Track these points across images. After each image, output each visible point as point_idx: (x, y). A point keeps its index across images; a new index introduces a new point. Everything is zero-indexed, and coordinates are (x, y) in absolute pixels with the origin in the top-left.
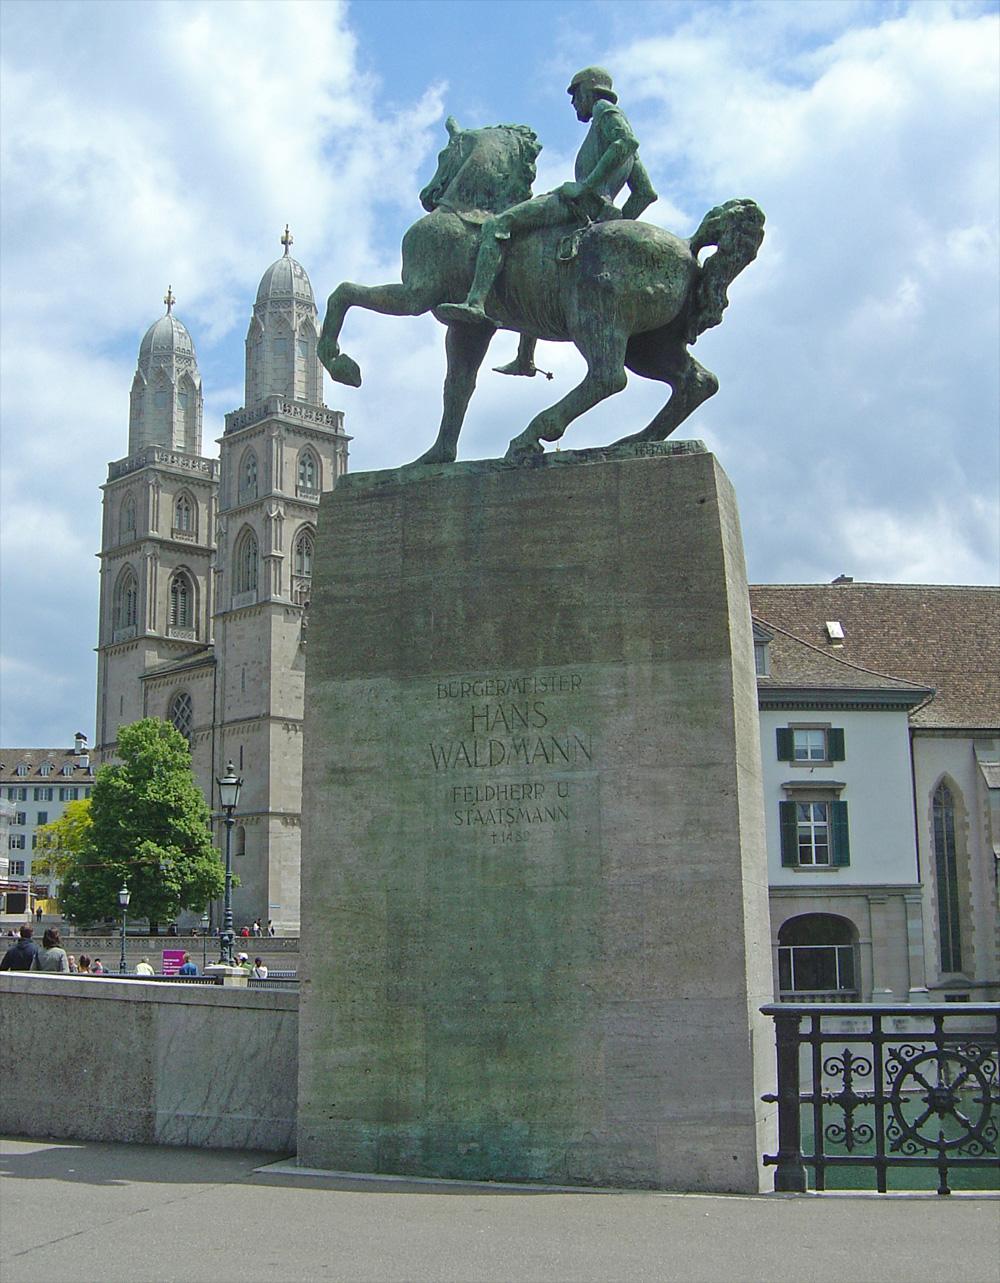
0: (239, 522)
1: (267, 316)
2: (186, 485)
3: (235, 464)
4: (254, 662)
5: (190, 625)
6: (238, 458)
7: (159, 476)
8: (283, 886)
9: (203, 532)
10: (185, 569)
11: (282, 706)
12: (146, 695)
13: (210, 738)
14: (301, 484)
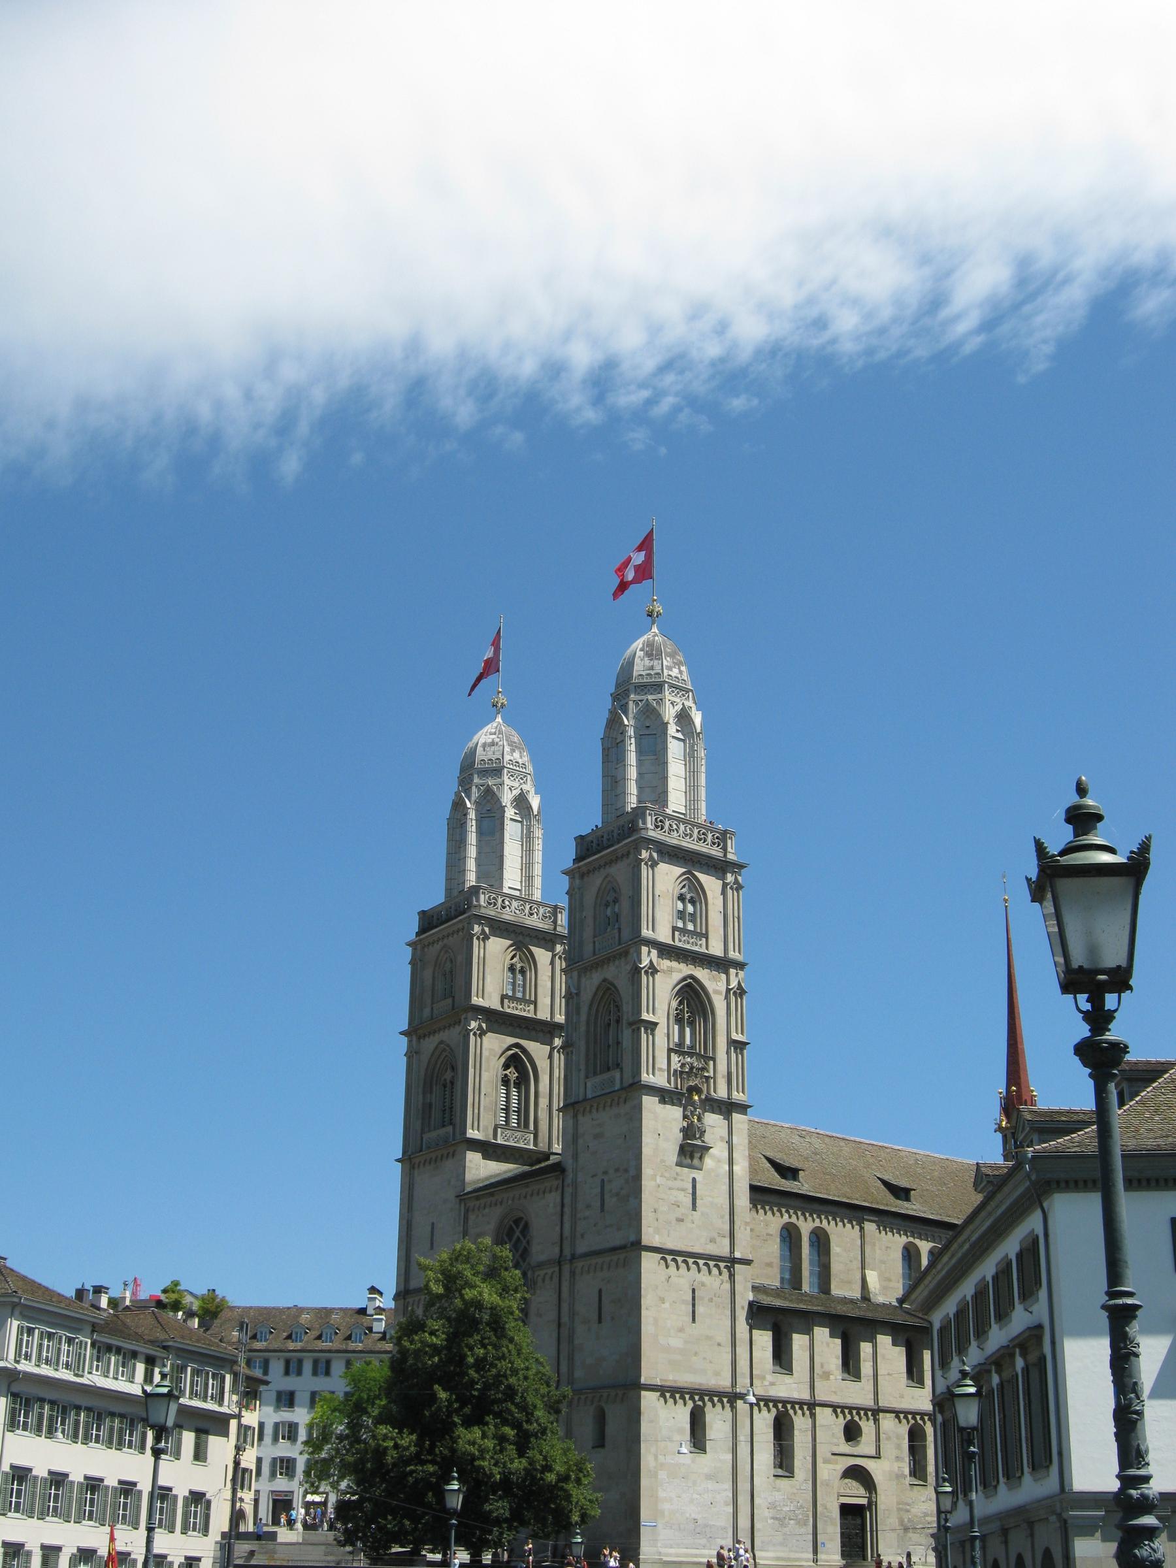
0: (596, 978)
1: (631, 703)
3: (590, 897)
4: (617, 1170)
5: (527, 1125)
6: (594, 890)
8: (661, 1494)
9: (544, 1001)
11: (657, 1231)
12: (466, 1219)
13: (556, 1280)
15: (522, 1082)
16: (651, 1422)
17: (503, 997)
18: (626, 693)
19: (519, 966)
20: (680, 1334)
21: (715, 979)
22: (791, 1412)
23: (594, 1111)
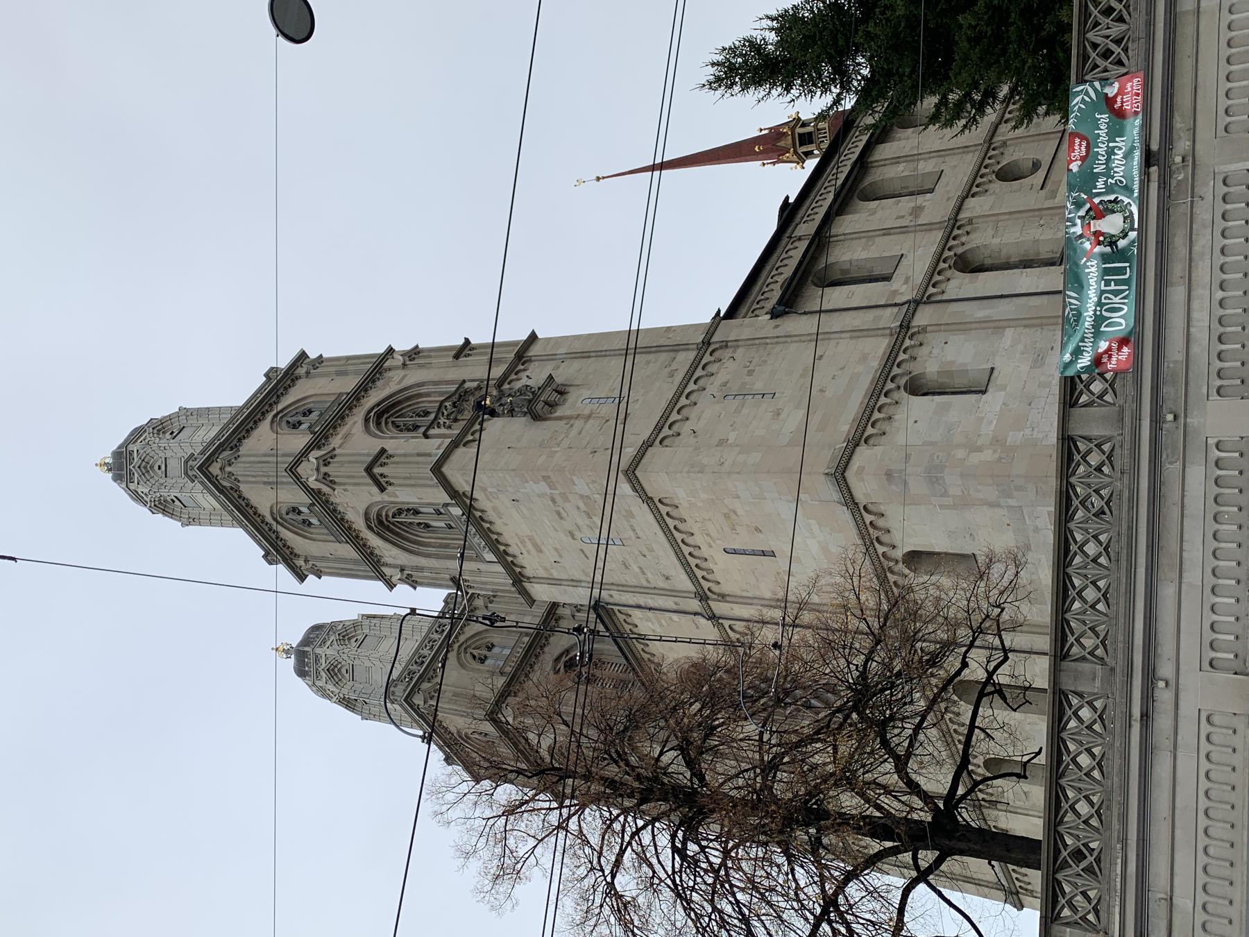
0: (374, 541)
2: (456, 646)
4: (559, 514)
7: (425, 686)
10: (564, 659)
16: (907, 457)
19: (485, 652)
20: (783, 415)
22: (960, 250)
23: (510, 550)
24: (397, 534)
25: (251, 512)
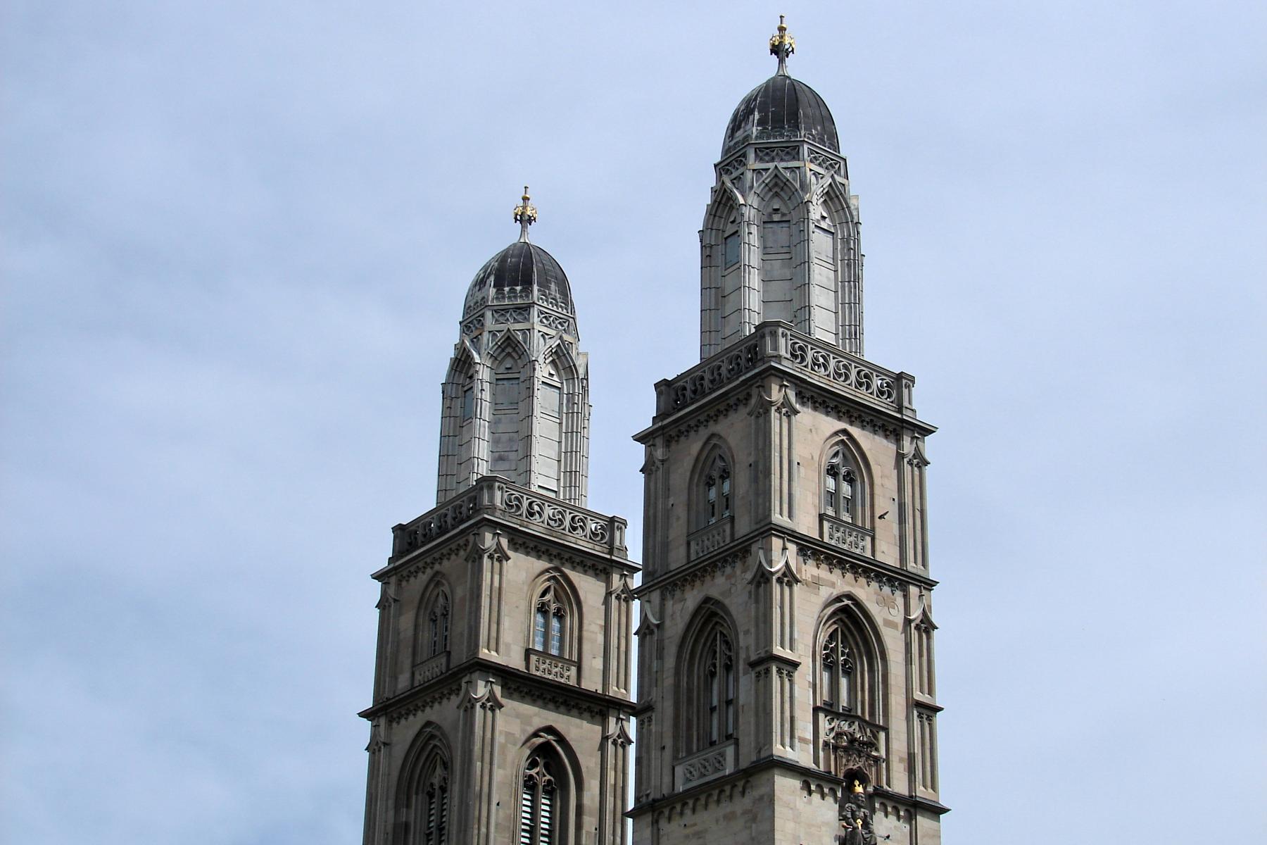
0: (692, 598)
1: (749, 175)
2: (556, 563)
6: (688, 463)
9: (593, 665)
14: (830, 512)
15: (557, 788)
17: (528, 652)
18: (741, 160)
19: (553, 607)
21: (886, 603)
23: (688, 812)
24: (701, 631)
25: (722, 407)
